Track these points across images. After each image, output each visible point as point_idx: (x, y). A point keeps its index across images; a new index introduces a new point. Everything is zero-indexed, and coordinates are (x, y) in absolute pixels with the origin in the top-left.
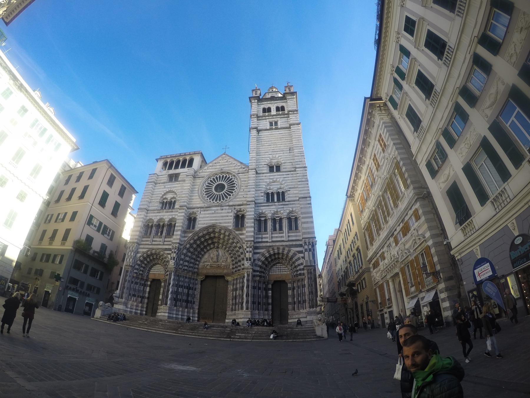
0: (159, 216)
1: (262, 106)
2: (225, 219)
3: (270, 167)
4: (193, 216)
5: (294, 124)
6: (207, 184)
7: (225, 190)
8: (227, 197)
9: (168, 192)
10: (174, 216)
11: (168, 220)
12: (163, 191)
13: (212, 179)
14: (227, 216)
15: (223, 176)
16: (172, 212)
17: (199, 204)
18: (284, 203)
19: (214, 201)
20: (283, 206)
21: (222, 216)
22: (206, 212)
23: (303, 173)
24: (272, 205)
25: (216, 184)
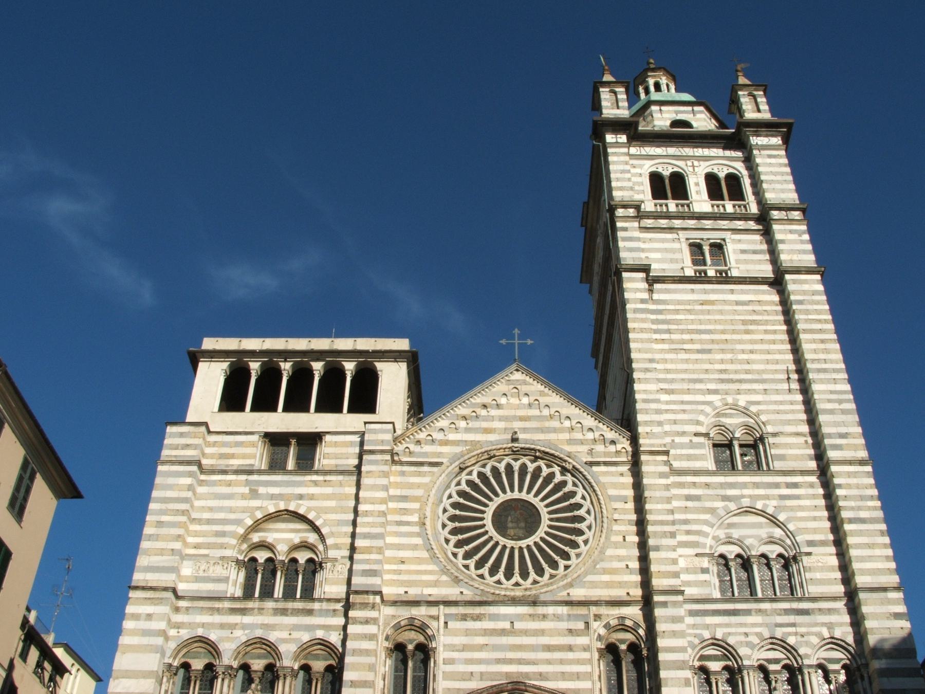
0: (244, 627)
1: (648, 167)
2: (562, 662)
3: (715, 445)
4: (412, 639)
5: (797, 271)
6: (456, 498)
7: (541, 533)
8: (554, 565)
9: (271, 517)
10: (320, 634)
11: (293, 648)
12: (252, 510)
13: (474, 477)
14: (570, 648)
15: (523, 468)
16: (310, 612)
17: (436, 584)
18: (795, 605)
19: (500, 575)
20: (791, 619)
21: (549, 648)
22: (471, 624)
23: (858, 487)
24: (748, 612)
25: (498, 501)
